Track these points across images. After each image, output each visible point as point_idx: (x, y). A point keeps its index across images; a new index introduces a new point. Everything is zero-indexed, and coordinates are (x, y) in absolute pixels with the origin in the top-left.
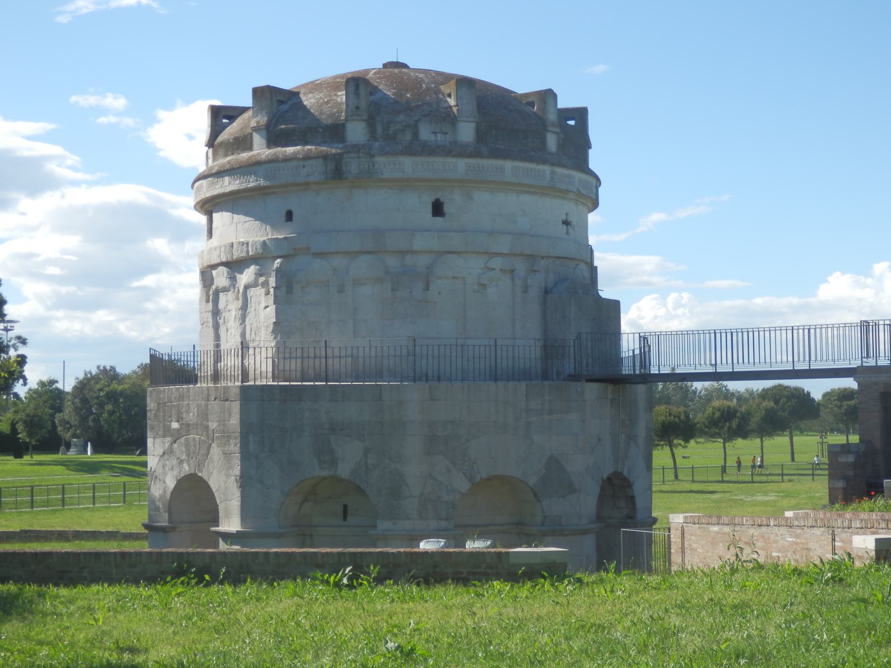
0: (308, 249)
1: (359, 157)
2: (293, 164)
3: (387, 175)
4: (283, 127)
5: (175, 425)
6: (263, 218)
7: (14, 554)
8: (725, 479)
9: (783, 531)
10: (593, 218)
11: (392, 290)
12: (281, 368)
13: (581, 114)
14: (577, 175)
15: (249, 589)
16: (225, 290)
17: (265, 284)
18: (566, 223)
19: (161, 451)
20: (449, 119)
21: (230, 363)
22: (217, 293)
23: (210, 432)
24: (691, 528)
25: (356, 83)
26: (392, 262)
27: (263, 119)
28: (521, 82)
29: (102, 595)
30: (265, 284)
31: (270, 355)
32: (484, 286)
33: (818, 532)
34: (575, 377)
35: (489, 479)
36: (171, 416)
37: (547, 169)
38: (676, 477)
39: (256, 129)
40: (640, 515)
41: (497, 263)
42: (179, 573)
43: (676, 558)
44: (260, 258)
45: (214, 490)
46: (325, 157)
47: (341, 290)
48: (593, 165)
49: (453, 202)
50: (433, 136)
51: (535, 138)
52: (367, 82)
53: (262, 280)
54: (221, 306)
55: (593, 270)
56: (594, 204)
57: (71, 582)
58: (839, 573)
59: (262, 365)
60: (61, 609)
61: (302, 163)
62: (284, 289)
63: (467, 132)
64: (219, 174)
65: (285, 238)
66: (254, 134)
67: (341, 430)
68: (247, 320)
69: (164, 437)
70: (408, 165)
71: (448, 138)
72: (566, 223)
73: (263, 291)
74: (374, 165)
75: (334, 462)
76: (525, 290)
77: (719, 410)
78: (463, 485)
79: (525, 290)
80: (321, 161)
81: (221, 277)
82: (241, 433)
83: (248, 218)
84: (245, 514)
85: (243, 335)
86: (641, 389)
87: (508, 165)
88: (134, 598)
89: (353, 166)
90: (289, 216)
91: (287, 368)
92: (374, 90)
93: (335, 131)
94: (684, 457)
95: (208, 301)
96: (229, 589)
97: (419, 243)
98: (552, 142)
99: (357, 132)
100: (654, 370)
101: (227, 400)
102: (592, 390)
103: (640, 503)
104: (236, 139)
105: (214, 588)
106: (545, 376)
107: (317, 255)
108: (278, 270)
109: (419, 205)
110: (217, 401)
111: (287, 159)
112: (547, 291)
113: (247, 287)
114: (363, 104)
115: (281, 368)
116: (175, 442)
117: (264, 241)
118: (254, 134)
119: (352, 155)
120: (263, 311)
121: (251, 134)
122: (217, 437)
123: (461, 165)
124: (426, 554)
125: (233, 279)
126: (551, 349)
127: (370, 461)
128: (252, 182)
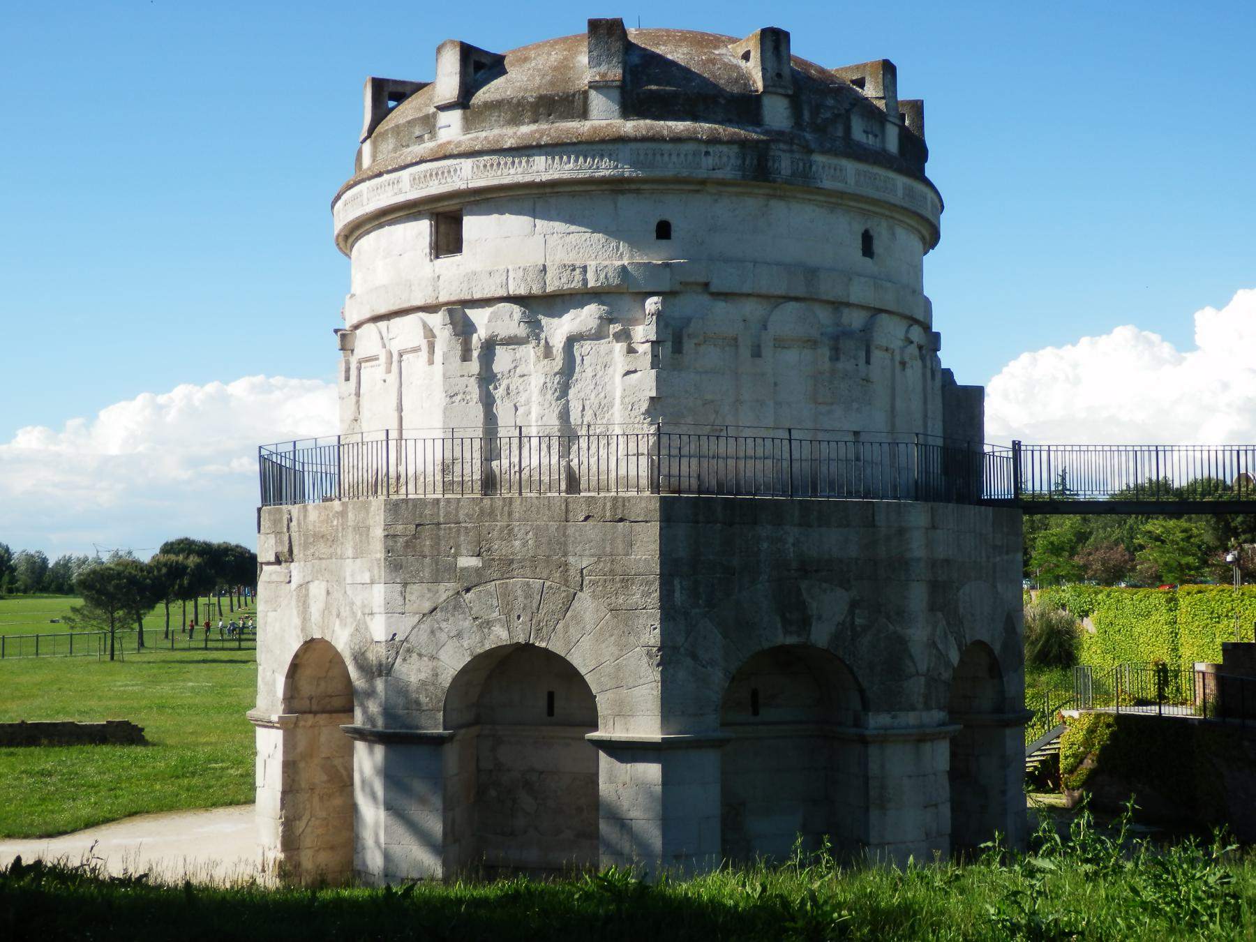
0: (706, 285)
1: (791, 151)
2: (690, 147)
3: (827, 184)
4: (654, 87)
6: (614, 231)
8: (176, 646)
11: (831, 359)
12: (622, 472)
16: (512, 341)
17: (624, 336)
19: (427, 606)
22: (489, 347)
23: (572, 572)
26: (824, 315)
30: (624, 336)
31: (643, 449)
36: (458, 547)
38: (141, 644)
39: (593, 86)
44: (616, 297)
45: (583, 671)
46: (743, 144)
47: (757, 353)
50: (864, 136)
53: (615, 328)
61: (703, 148)
62: (669, 344)
65: (666, 265)
66: (593, 93)
67: (816, 571)
68: (572, 392)
69: (436, 581)
73: (619, 348)
74: (811, 166)
75: (805, 623)
77: (165, 565)
80: (735, 149)
82: (661, 575)
83: (573, 228)
84: (669, 707)
85: (564, 415)
89: (784, 164)
90: (664, 230)
91: (675, 471)
93: (742, 106)
94: (53, 621)
95: (466, 357)
99: (777, 113)
101: (621, 520)
104: (541, 98)
108: (659, 315)
110: (590, 522)
111: (677, 139)
113: (571, 341)
115: (622, 472)
116: (468, 590)
117: (624, 267)
118: (593, 94)
119: (782, 146)
120: (620, 380)
121: (585, 93)
122: (594, 583)
127: (858, 621)
128: (605, 169)
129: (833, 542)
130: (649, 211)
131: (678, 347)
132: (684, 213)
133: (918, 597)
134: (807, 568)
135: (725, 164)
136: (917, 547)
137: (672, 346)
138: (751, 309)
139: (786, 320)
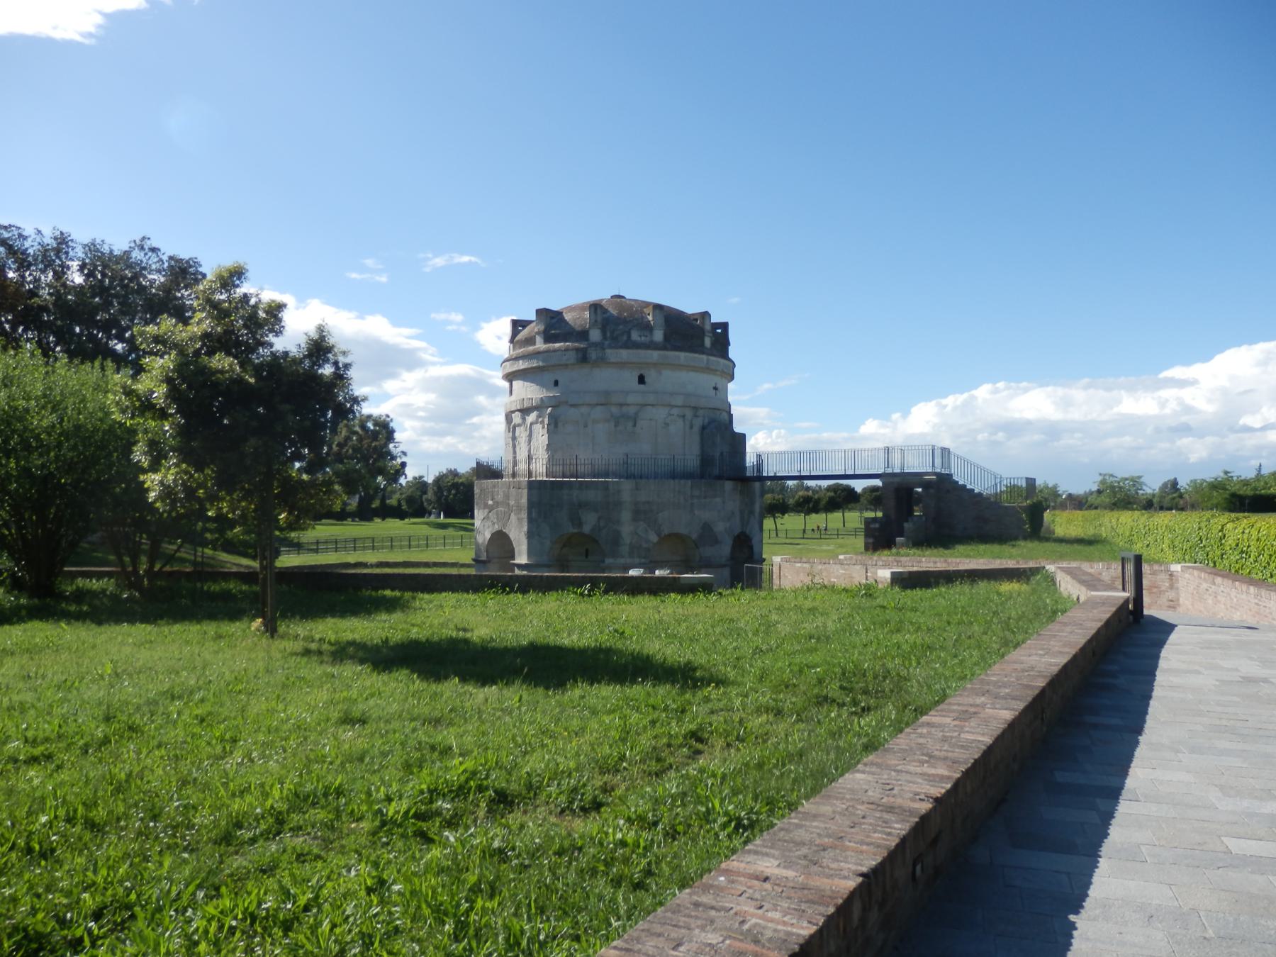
3: (613, 360)
5: (490, 502)
6: (541, 384)
7: (399, 575)
9: (838, 566)
10: (731, 386)
13: (725, 326)
14: (722, 361)
15: (531, 596)
16: (519, 425)
17: (542, 422)
18: (715, 388)
20: (648, 328)
21: (522, 467)
24: (785, 565)
25: (595, 307)
26: (614, 410)
27: (542, 327)
28: (689, 306)
29: (448, 598)
30: (542, 422)
32: (667, 424)
33: (858, 567)
34: (720, 478)
35: (670, 535)
37: (704, 357)
40: (756, 557)
41: (675, 411)
42: (491, 587)
43: (776, 581)
44: (539, 407)
46: (577, 349)
47: (586, 426)
48: (731, 355)
49: (651, 376)
51: (699, 339)
52: (601, 307)
54: (517, 434)
55: (731, 416)
56: (732, 378)
57: (431, 590)
58: (869, 591)
59: (540, 469)
60: (425, 606)
63: (658, 336)
64: (516, 359)
70: (625, 354)
71: (648, 339)
72: (715, 388)
75: (580, 524)
76: (691, 427)
78: (654, 538)
79: (691, 427)
81: (517, 418)
84: (530, 553)
86: (757, 485)
87: (682, 355)
88: (466, 600)
89: (593, 354)
90: (556, 383)
92: (605, 311)
93: (583, 335)
96: (520, 596)
97: (630, 399)
98: (708, 342)
99: (595, 335)
100: (765, 474)
102: (729, 485)
103: (756, 549)
105: (512, 596)
106: (702, 476)
107: (572, 406)
109: (630, 378)
111: (555, 351)
112: (703, 428)
114: (599, 319)
120: (541, 437)
123: (655, 355)
124: (632, 577)
125: (524, 419)
126: (706, 460)
128: (535, 364)
129: (591, 495)
130: (550, 377)
131: (556, 425)
132: (562, 376)
133: (626, 515)
134: (582, 505)
135: (572, 357)
136: (626, 496)
137: (554, 426)
138: (584, 410)
139: (598, 412)
